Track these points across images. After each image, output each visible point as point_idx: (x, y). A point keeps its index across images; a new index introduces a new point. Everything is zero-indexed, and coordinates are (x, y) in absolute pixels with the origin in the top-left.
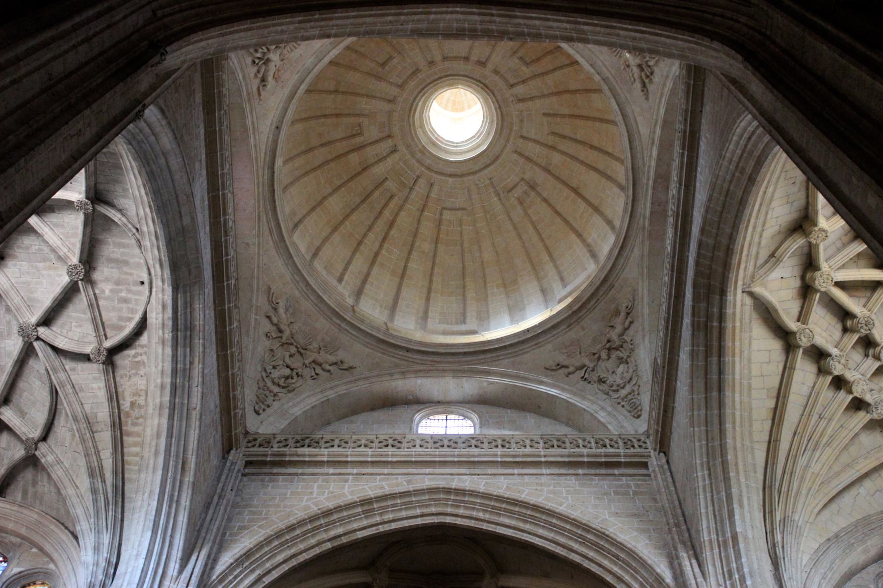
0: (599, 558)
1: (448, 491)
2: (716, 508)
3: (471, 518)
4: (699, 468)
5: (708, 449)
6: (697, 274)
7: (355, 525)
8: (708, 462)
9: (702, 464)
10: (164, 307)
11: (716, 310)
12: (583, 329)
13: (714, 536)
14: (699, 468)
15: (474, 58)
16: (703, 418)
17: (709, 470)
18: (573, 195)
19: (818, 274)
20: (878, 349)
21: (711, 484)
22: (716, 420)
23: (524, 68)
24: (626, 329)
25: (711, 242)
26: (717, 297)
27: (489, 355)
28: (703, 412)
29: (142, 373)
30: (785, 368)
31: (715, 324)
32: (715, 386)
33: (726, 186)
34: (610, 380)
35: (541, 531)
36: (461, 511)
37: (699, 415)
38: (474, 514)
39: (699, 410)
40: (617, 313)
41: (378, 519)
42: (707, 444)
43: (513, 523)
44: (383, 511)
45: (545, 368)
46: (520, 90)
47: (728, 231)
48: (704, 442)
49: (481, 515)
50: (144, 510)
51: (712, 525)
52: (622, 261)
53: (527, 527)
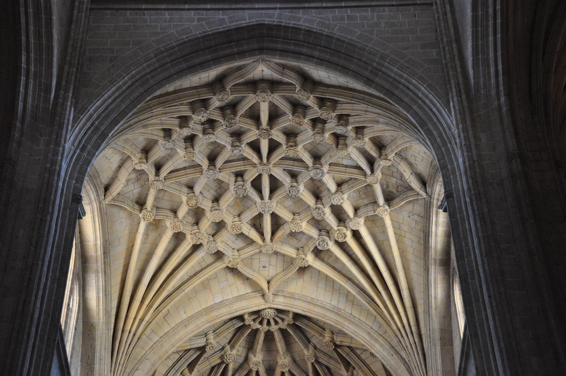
0: (31, 20)
2: (112, 106)
4: (130, 75)
5: (145, 75)
6: (270, 27)
8: (136, 81)
9: (133, 76)
13: (95, 116)
14: (130, 75)
17: (132, 84)
19: (269, 93)
20: (210, 131)
21: (124, 91)
22: (167, 73)
26: (256, 46)
28: (168, 60)
30: (196, 88)
31: (235, 50)
33: (356, 56)
42: (147, 74)
47: (316, 54)
48: (148, 70)
51: (101, 110)
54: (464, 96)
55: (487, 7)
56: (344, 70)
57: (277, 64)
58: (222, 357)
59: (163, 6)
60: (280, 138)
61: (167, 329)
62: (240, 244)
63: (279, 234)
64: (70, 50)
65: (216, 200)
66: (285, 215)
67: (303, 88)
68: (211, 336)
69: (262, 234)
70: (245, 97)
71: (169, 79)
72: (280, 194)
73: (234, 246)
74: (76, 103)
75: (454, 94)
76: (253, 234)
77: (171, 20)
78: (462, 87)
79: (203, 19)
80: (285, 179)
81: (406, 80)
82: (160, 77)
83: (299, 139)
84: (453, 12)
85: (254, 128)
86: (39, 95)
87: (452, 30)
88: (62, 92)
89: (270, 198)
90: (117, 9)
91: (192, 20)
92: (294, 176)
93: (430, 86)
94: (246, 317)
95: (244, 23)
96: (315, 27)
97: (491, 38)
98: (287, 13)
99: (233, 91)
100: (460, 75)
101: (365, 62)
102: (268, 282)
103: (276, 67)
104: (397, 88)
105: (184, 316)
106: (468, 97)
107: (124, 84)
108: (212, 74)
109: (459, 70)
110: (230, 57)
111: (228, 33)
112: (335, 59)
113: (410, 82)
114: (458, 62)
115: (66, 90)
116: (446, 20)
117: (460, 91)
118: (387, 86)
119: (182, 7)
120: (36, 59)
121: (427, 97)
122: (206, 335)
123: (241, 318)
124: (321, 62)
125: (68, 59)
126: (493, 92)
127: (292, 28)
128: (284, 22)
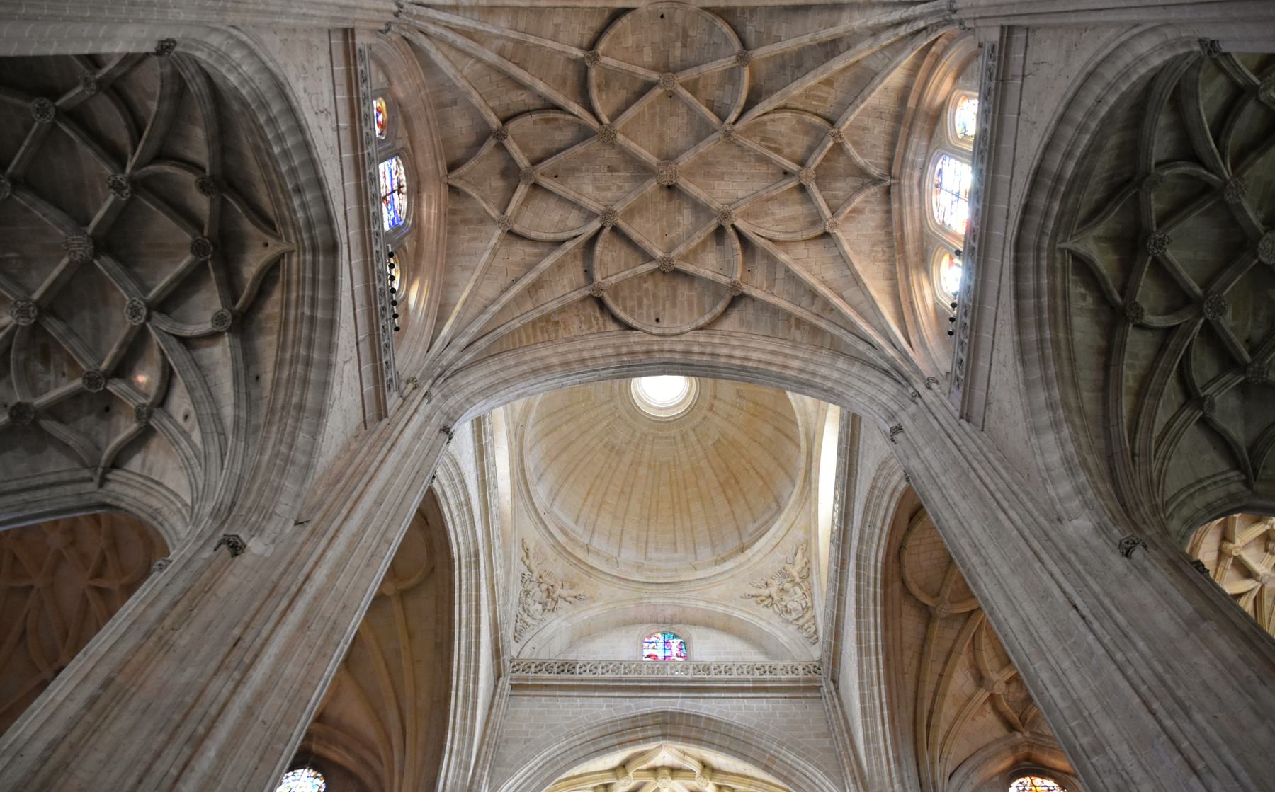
3: (460, 581)
6: (673, 714)
7: (452, 502)
8: (547, 762)
10: (648, 352)
11: (650, 733)
12: (555, 560)
15: (716, 403)
16: (573, 744)
18: (619, 490)
19: (669, 779)
22: (575, 757)
23: (710, 442)
24: (565, 599)
25: (702, 725)
26: (659, 732)
27: (523, 488)
28: (578, 743)
29: (583, 327)
30: (600, 772)
31: (640, 735)
32: (598, 747)
33: (753, 743)
34: (529, 600)
35: (463, 642)
36: (464, 571)
37: (574, 741)
38: (464, 582)
39: (579, 739)
40: (573, 586)
41: (455, 513)
43: (464, 616)
44: (461, 516)
46: (693, 438)
47: (717, 741)
48: (558, 752)
49: (464, 587)
50: (492, 379)
52: (609, 578)
53: (464, 629)
54: (859, 784)
55: (874, 700)
56: (743, 757)
57: (679, 750)
59: (576, 694)
64: (489, 731)
67: (702, 774)
70: (645, 783)
71: (576, 762)
74: (491, 781)
75: (850, 781)
77: (582, 706)
78: (857, 774)
79: (611, 706)
81: (803, 767)
82: (571, 759)
84: (841, 706)
86: (459, 772)
87: (842, 721)
88: (479, 770)
90: (534, 696)
91: (601, 707)
93: (826, 773)
95: (649, 710)
96: (715, 715)
97: (880, 728)
98: (688, 702)
99: (635, 777)
100: (854, 764)
101: (764, 750)
103: (677, 753)
104: (794, 775)
106: (863, 784)
107: (536, 765)
108: (615, 759)
109: (852, 758)
110: (635, 742)
111: (633, 719)
112: (734, 747)
113: (807, 770)
114: (850, 751)
115: (484, 769)
116: (836, 713)
117: (855, 778)
118: (785, 773)
119: (592, 694)
120: (459, 739)
121: (824, 784)
124: (720, 748)
125: (487, 739)
126: (887, 779)
127: (694, 715)
128: (686, 710)
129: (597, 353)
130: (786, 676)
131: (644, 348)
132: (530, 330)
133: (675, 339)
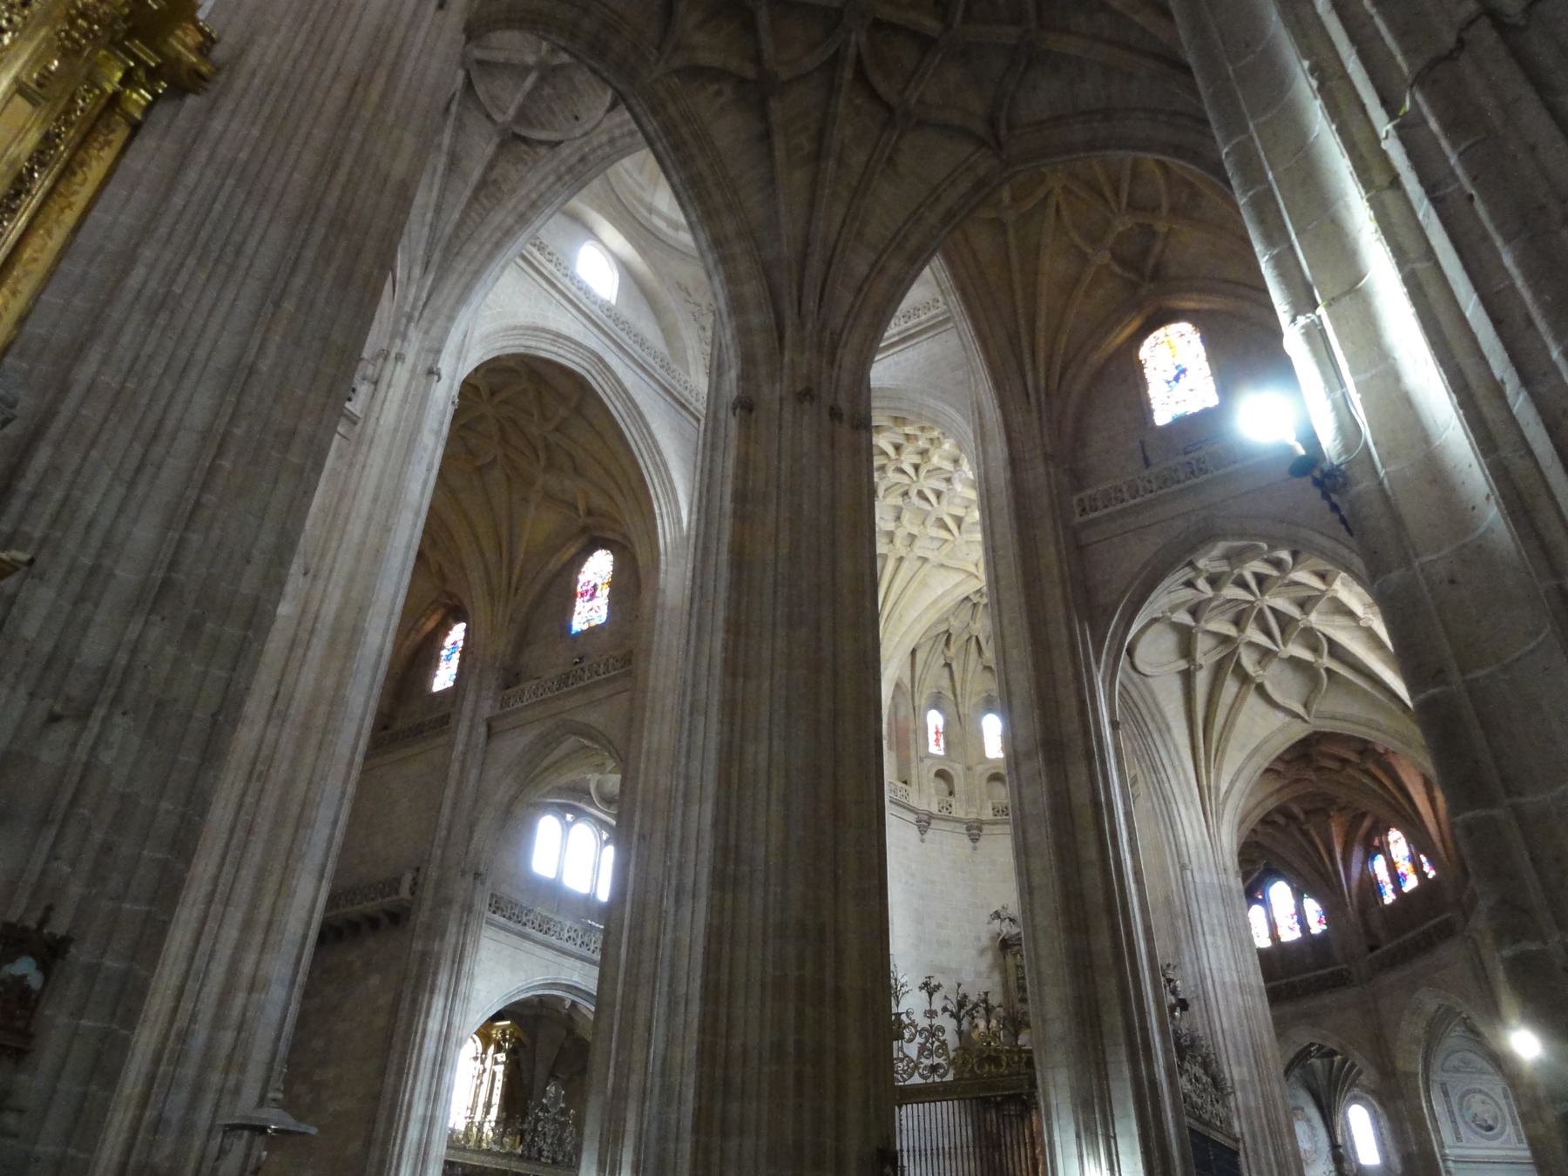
1: (601, 360)
3: (601, 386)
7: (543, 346)
36: (599, 379)
38: (605, 386)
41: (555, 349)
45: (678, 283)
49: (608, 391)
50: (463, 280)
53: (628, 421)
58: (969, 632)
60: (916, 459)
61: (904, 629)
62: (936, 544)
63: (963, 526)
65: (898, 518)
66: (960, 512)
68: (952, 619)
69: (949, 530)
72: (944, 501)
73: (932, 547)
76: (943, 534)
80: (942, 486)
83: (930, 454)
85: (885, 462)
89: (939, 503)
92: (948, 480)
94: (971, 597)
102: (976, 565)
105: (916, 615)
122: (947, 619)
123: (967, 598)
129: (543, 187)
130: (930, 314)
131: (577, 157)
132: (477, 206)
133: (598, 130)
